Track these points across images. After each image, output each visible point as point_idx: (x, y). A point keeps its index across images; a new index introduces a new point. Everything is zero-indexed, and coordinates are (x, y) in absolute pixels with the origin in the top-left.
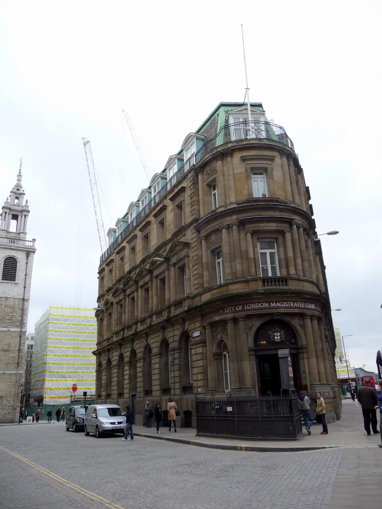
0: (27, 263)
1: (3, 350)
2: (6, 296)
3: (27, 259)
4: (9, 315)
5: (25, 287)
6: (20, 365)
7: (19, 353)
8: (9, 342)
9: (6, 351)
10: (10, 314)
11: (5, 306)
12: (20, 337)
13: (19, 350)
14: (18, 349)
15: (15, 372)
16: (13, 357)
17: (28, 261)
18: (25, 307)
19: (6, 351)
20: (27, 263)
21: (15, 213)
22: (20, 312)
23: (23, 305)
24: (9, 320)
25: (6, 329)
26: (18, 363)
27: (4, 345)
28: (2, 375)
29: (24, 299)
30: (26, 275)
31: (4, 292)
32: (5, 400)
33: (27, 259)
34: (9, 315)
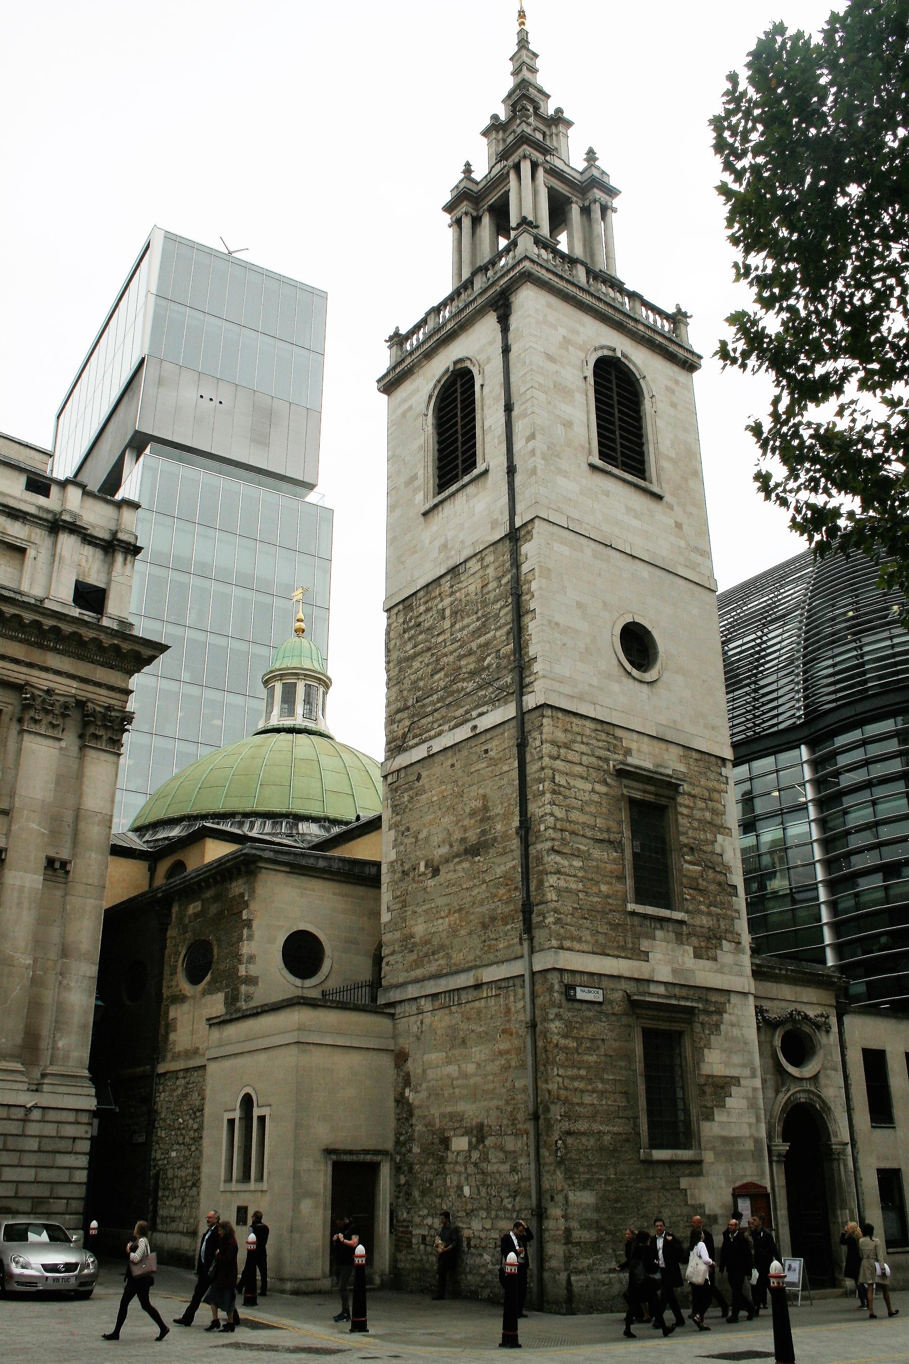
0: (506, 350)
1: (466, 852)
2: (451, 563)
3: (505, 330)
4: (470, 653)
5: (511, 470)
6: (535, 919)
7: (526, 845)
8: (484, 797)
9: (473, 851)
10: (474, 645)
11: (454, 613)
12: (522, 746)
13: (526, 828)
14: (516, 823)
15: (517, 968)
16: (507, 878)
17: (511, 336)
18: (525, 568)
19: (473, 851)
20: (506, 350)
21: (492, 199)
22: (506, 615)
23: (516, 563)
24: (473, 674)
25: (464, 732)
26: (527, 909)
27: (467, 822)
28: (472, 994)
29: (515, 536)
30: (509, 408)
31: (444, 547)
32: (495, 1147)
33: (505, 330)
34: (470, 653)
